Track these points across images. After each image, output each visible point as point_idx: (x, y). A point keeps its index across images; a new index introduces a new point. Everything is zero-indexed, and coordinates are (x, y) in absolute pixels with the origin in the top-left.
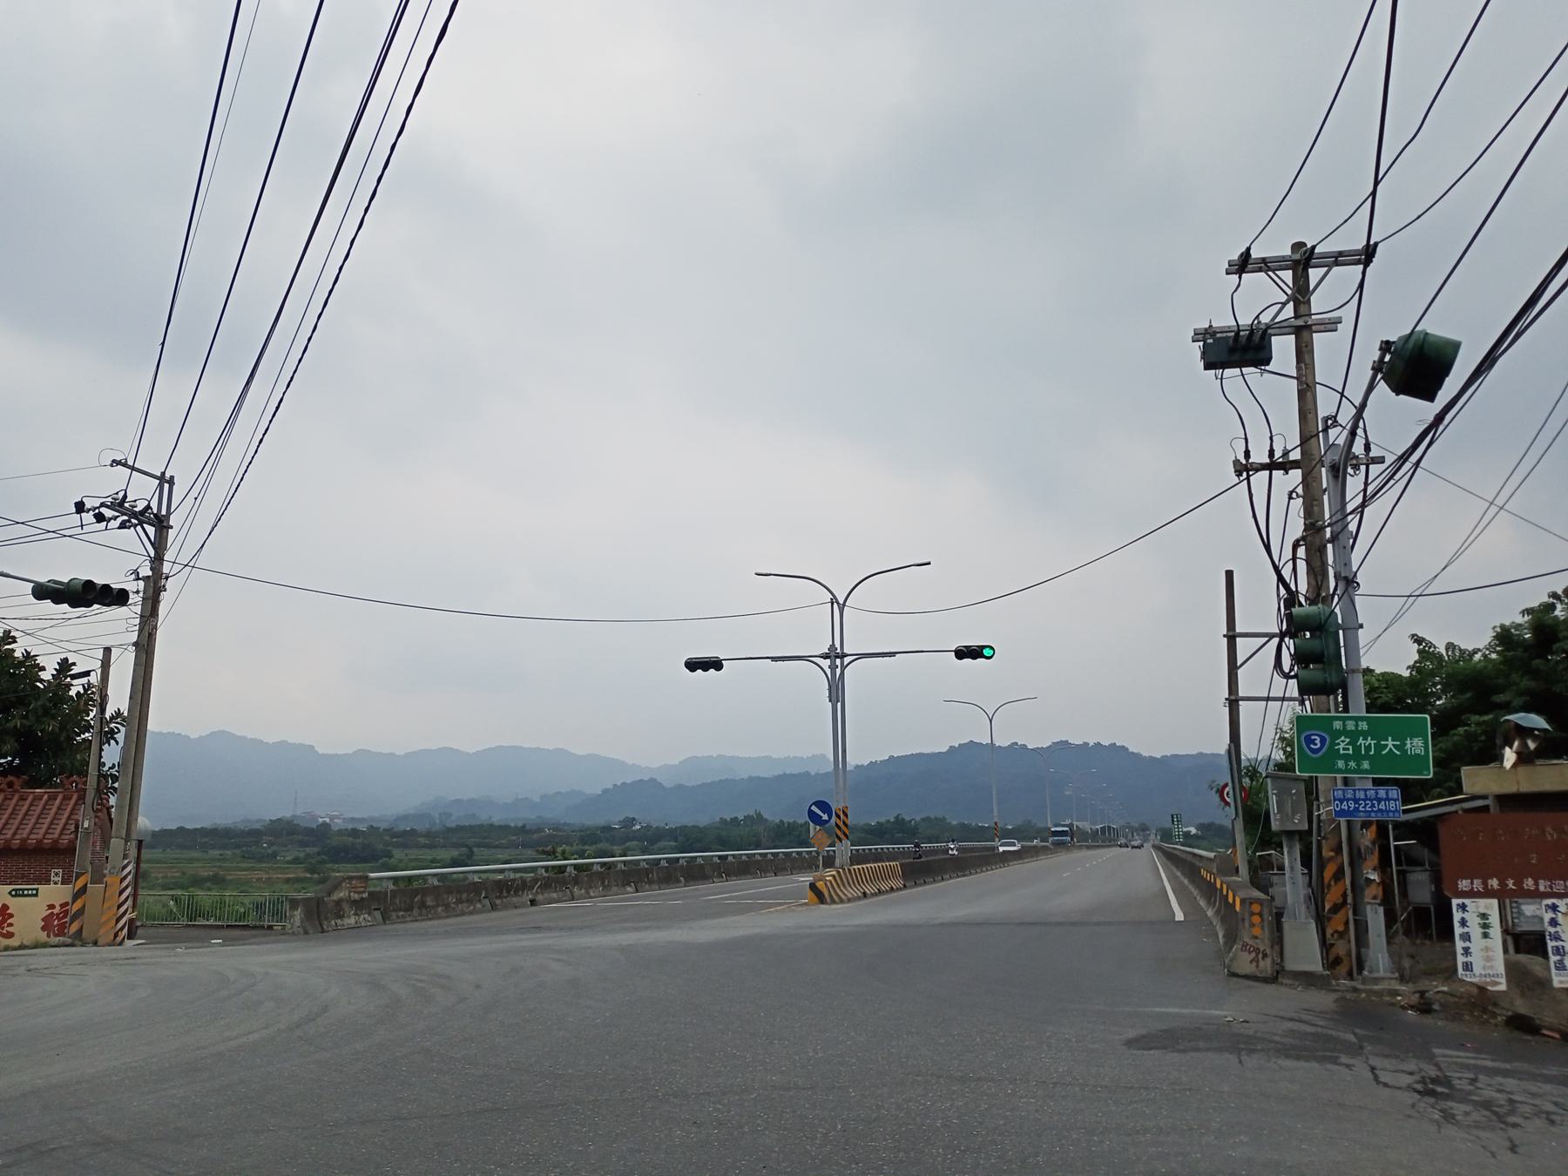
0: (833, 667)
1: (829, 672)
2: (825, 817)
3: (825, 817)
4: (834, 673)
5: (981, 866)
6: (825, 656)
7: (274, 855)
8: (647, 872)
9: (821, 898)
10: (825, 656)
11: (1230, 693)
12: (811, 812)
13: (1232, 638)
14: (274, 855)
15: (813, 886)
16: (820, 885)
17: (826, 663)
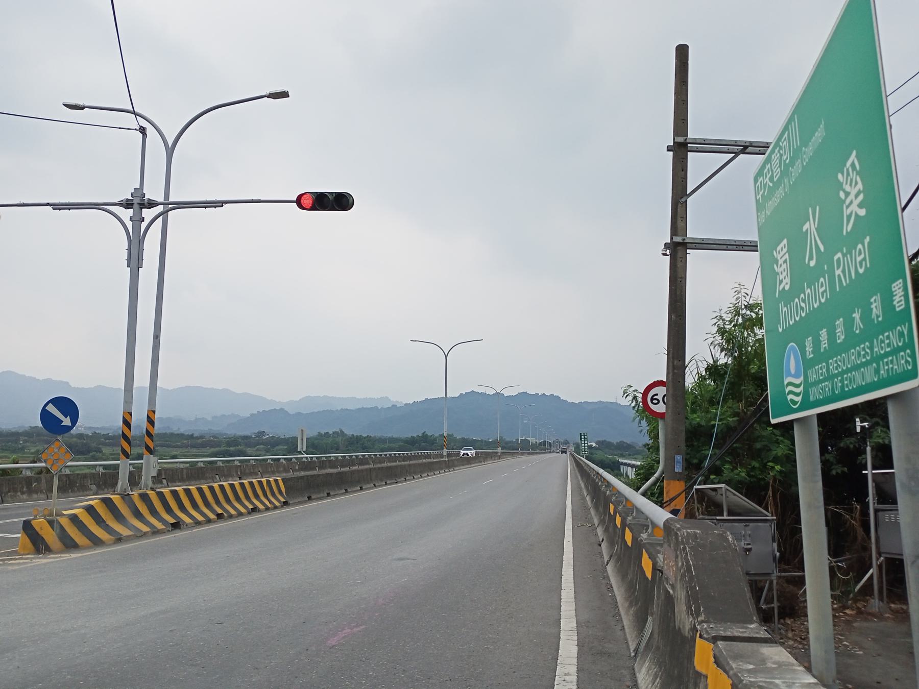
0: (138, 220)
1: (130, 225)
2: (67, 422)
3: (67, 422)
4: (137, 228)
5: (422, 472)
6: (127, 205)
7: (23, 449)
8: (29, 481)
9: (39, 545)
10: (127, 205)
11: (674, 231)
12: (45, 415)
13: (680, 149)
14: (23, 449)
15: (27, 527)
16: (40, 524)
17: (126, 214)
